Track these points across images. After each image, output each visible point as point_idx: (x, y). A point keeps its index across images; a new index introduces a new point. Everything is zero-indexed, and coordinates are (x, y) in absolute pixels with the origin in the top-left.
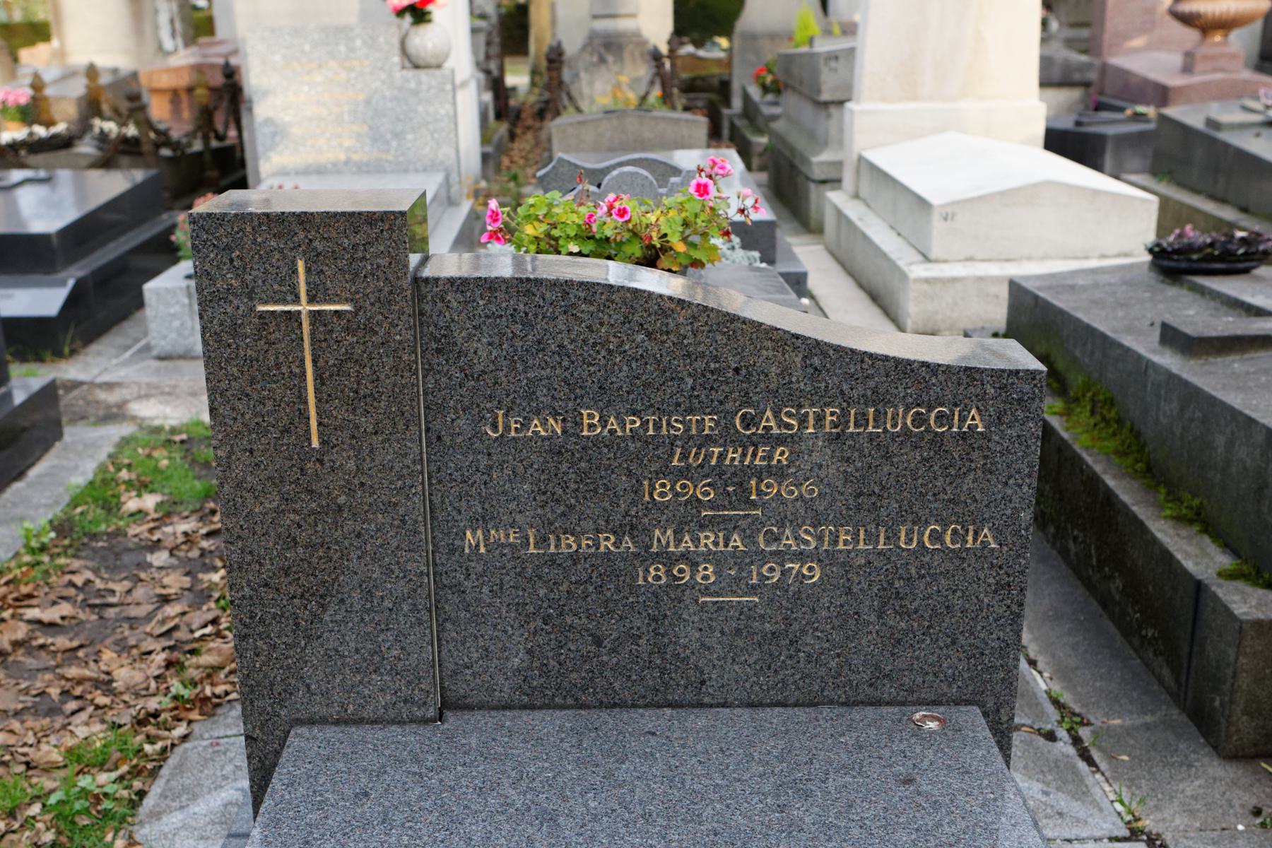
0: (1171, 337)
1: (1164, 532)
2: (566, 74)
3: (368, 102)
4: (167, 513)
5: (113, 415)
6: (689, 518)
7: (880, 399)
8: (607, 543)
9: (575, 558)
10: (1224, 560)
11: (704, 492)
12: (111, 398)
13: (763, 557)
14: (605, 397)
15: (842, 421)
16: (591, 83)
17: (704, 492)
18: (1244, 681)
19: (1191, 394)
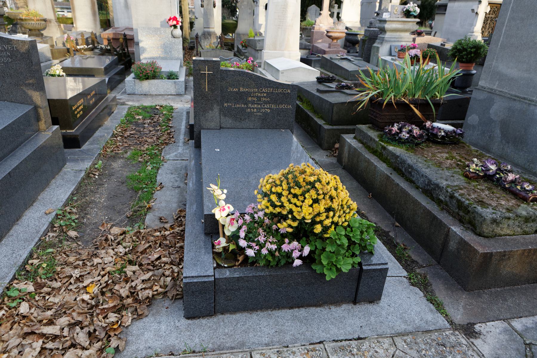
0: (318, 91)
1: (316, 119)
2: (199, 40)
3: (164, 44)
4: (144, 119)
5: (123, 104)
6: (253, 103)
7: (277, 88)
8: (243, 106)
9: (239, 108)
10: (324, 122)
11: (255, 99)
12: (121, 101)
13: (263, 108)
14: (243, 86)
15: (273, 91)
16: (204, 43)
17: (255, 99)
18: (326, 138)
19: (320, 99)
